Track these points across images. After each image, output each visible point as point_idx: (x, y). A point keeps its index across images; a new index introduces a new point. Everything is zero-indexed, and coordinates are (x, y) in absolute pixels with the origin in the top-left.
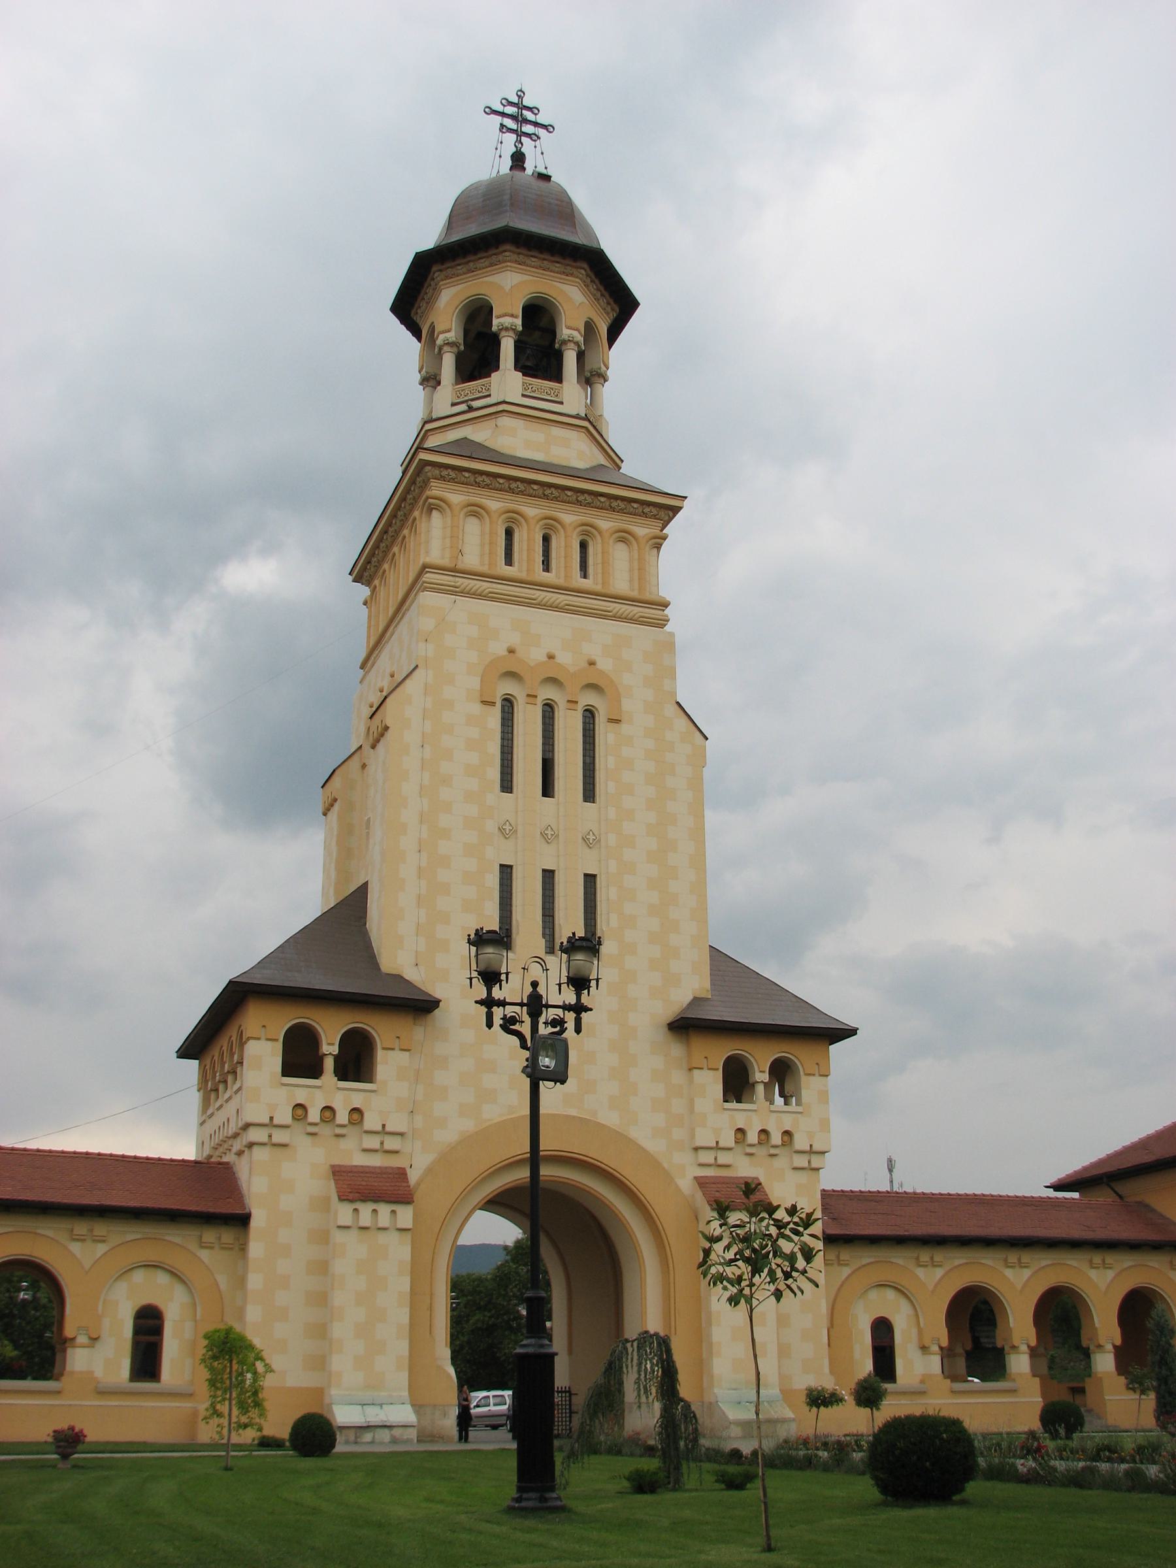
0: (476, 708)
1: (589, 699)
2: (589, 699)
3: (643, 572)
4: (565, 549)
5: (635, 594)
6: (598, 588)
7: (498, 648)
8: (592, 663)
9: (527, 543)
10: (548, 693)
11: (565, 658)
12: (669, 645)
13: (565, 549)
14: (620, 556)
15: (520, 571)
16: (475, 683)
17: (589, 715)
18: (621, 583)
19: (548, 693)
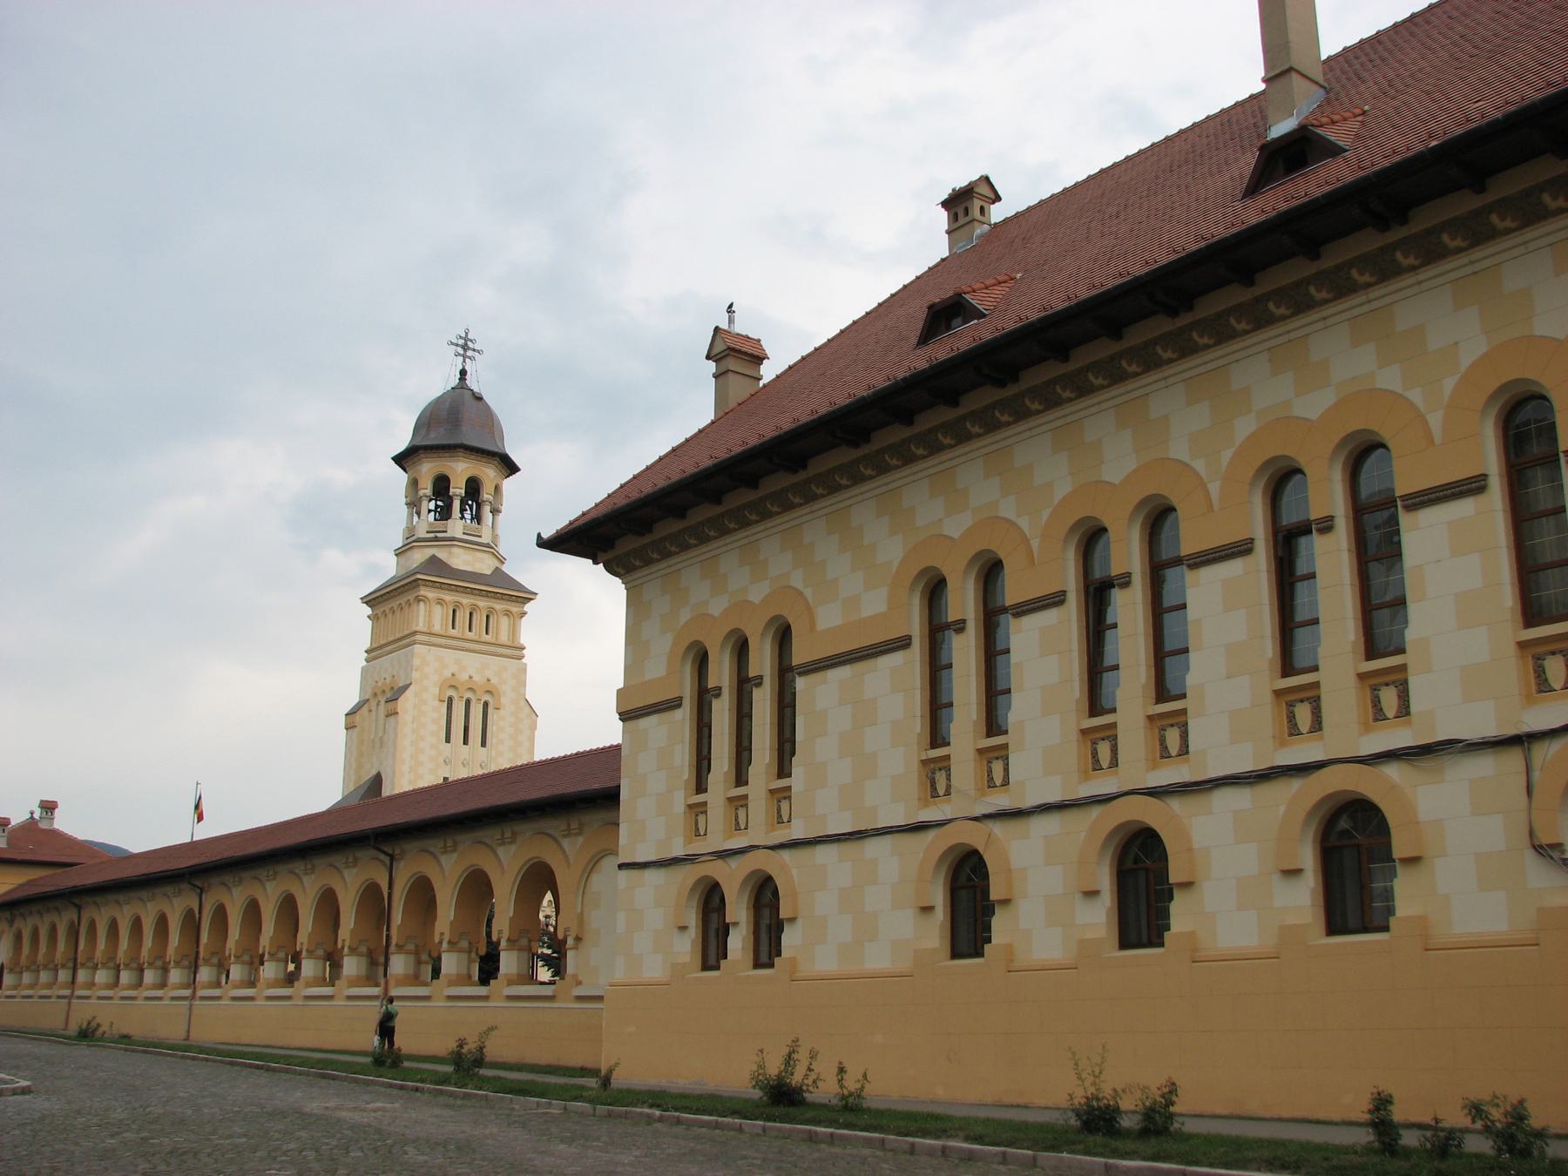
0: (436, 703)
1: (487, 697)
2: (487, 697)
3: (514, 631)
4: (479, 620)
5: (509, 643)
6: (493, 641)
7: (447, 673)
8: (489, 680)
9: (463, 617)
10: (469, 695)
11: (476, 678)
12: (524, 670)
13: (479, 620)
14: (504, 621)
15: (458, 632)
16: (437, 691)
17: (486, 705)
18: (504, 638)
19: (469, 695)
